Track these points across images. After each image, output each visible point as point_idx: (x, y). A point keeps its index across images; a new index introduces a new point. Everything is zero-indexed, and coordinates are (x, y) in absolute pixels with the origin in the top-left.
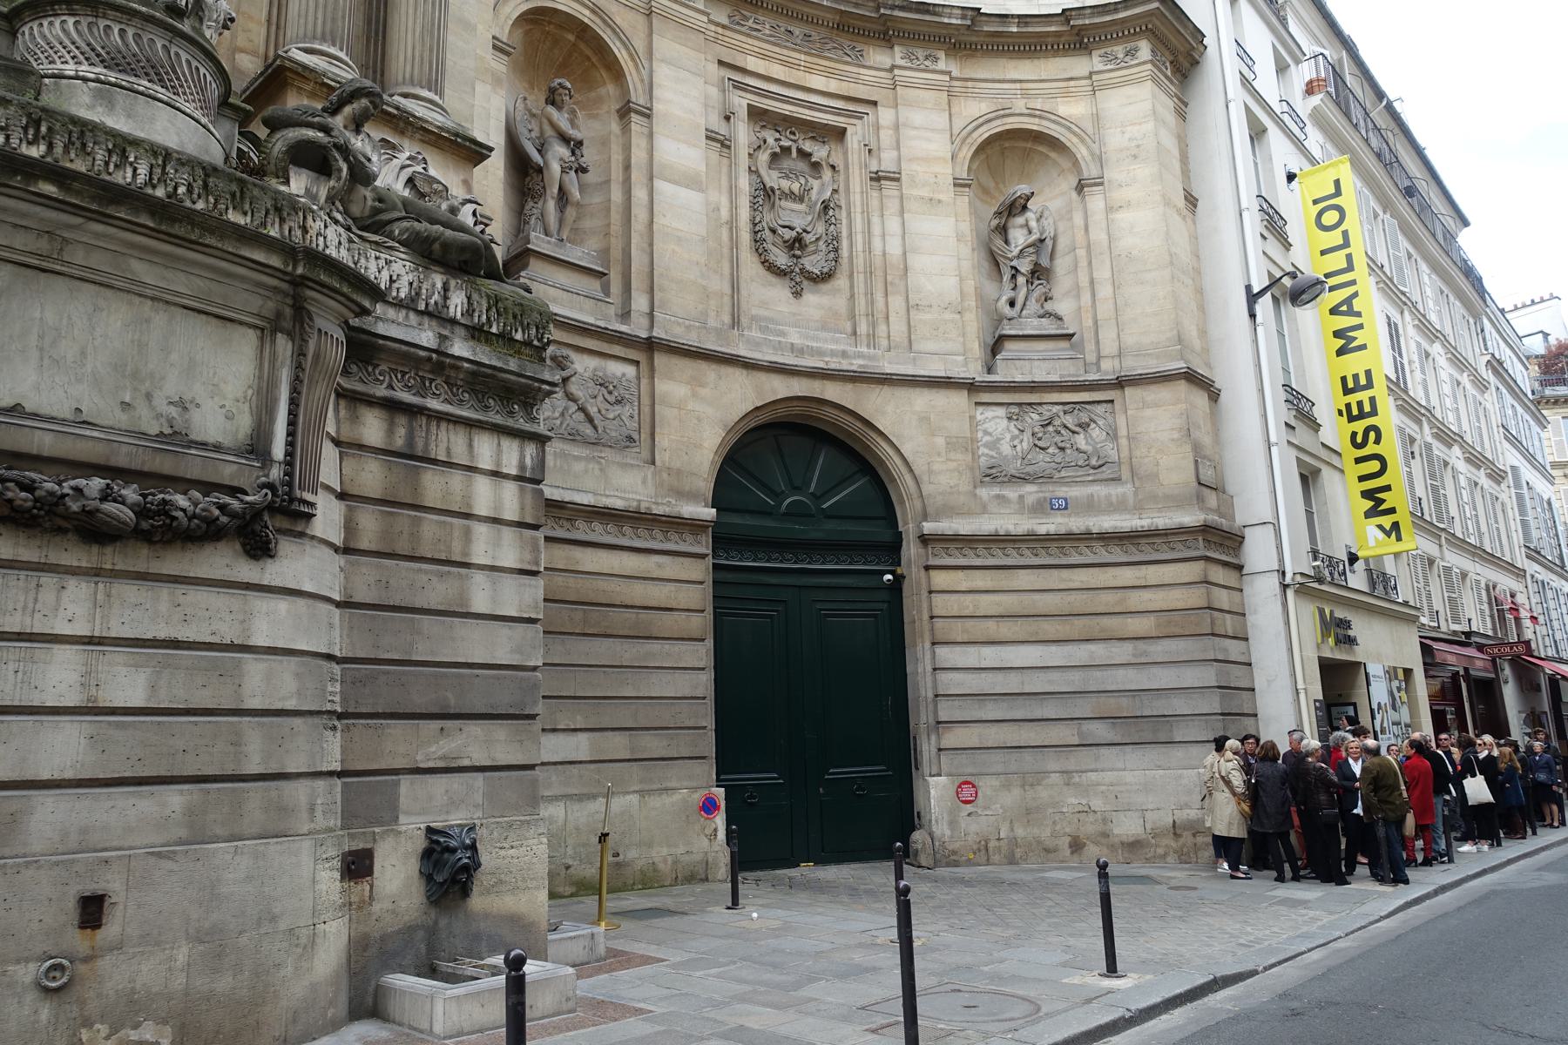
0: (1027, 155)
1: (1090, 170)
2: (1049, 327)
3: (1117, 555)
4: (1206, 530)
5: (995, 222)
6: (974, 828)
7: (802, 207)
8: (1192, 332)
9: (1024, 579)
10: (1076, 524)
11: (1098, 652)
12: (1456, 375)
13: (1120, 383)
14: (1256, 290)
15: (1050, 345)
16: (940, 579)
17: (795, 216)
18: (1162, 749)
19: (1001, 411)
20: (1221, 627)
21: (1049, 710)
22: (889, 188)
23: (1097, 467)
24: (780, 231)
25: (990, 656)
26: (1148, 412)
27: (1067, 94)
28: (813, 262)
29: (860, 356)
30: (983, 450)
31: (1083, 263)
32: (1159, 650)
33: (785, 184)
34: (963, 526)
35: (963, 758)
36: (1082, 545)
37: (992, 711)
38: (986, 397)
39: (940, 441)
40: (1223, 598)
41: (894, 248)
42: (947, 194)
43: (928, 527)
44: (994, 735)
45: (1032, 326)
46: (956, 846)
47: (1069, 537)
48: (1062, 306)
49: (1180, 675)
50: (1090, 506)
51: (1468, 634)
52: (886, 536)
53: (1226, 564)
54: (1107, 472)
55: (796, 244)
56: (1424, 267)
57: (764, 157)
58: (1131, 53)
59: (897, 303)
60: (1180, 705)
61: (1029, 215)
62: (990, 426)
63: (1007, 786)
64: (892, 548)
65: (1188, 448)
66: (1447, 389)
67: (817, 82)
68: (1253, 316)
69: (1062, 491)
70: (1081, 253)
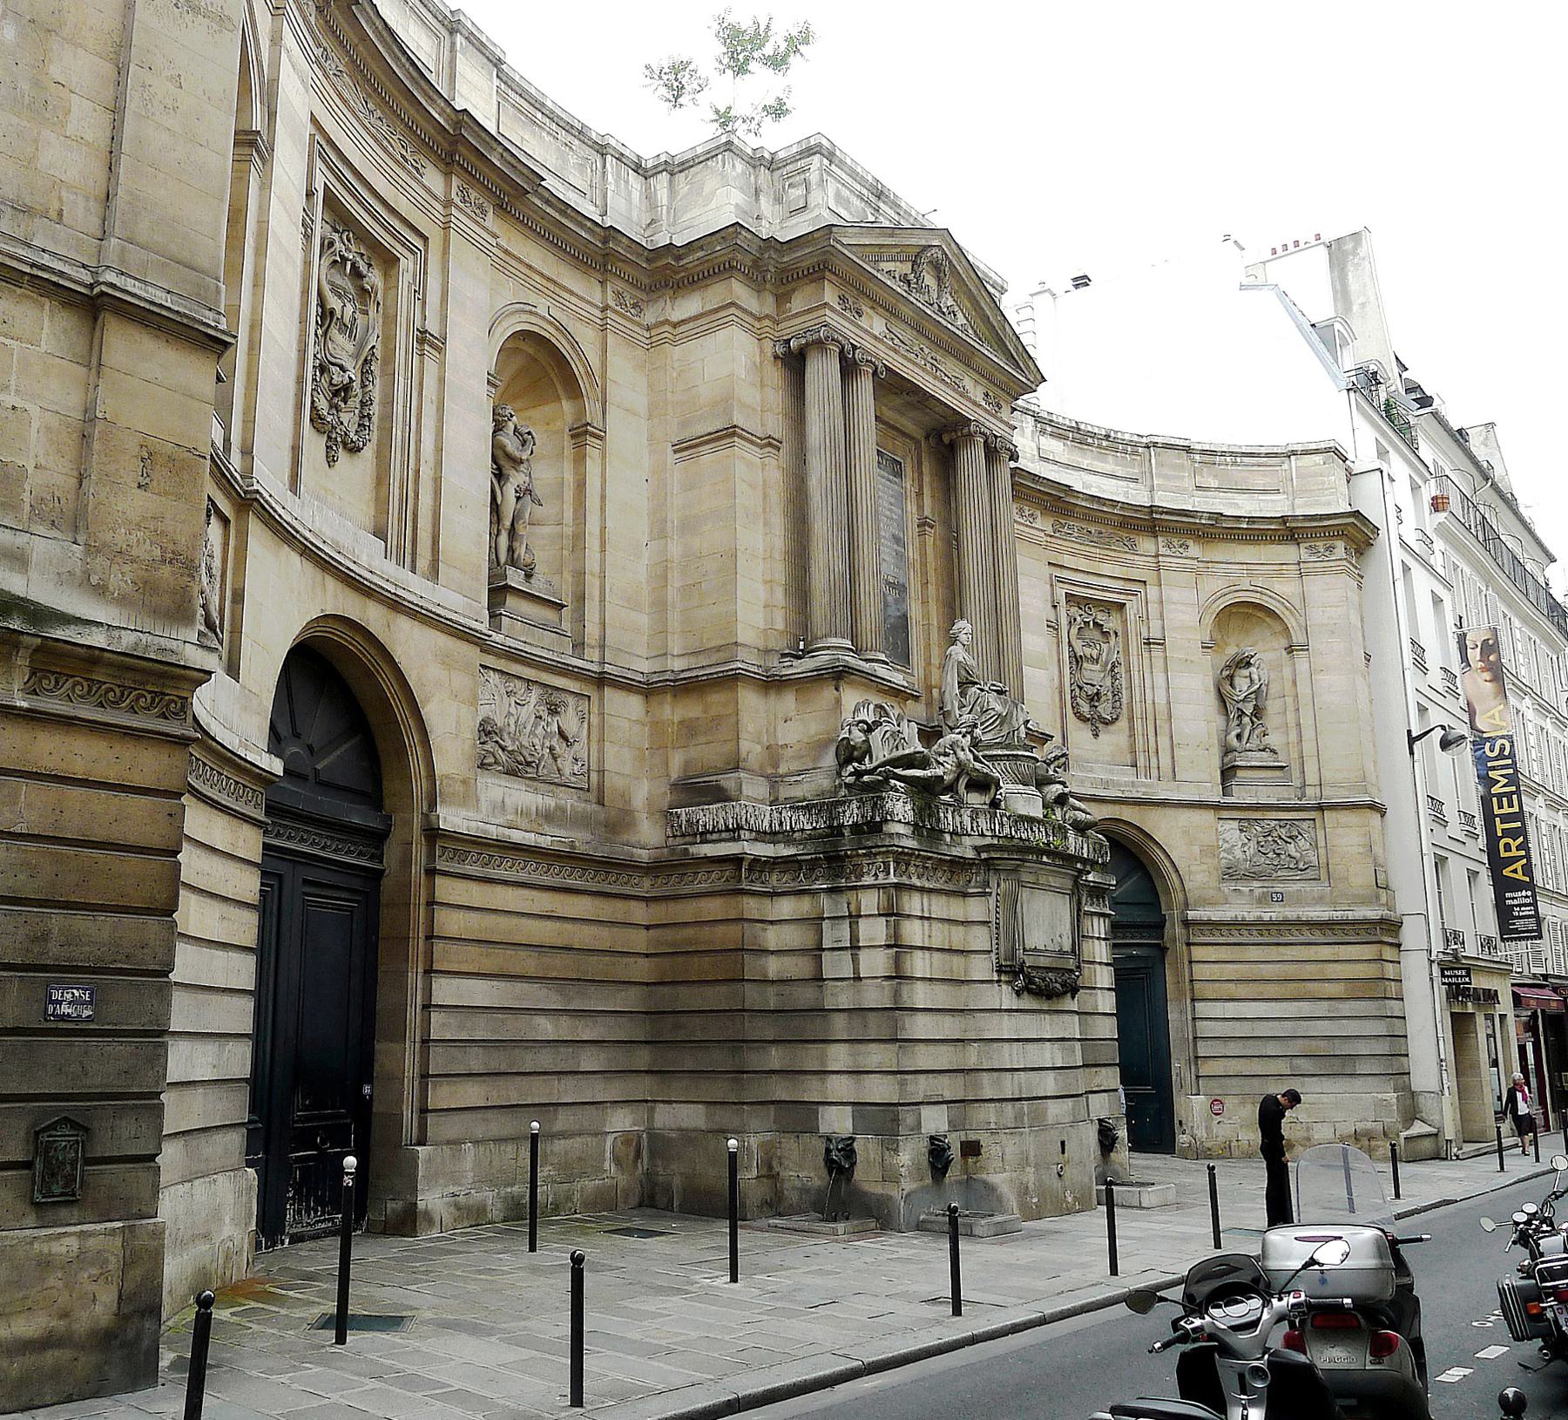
0: (1249, 616)
1: (1298, 638)
2: (1265, 759)
3: (1318, 937)
4: (1382, 921)
5: (1226, 673)
6: (1221, 1133)
7: (1098, 667)
8: (1370, 767)
9: (1253, 953)
10: (1290, 913)
11: (1305, 1008)
12: (1541, 722)
13: (1321, 808)
14: (1414, 734)
15: (1269, 773)
16: (1198, 953)
17: (1093, 673)
18: (1348, 1079)
19: (1235, 824)
20: (1380, 990)
21: (1272, 1049)
22: (1157, 652)
23: (1300, 868)
24: (1086, 688)
25: (1231, 1009)
26: (1340, 831)
27: (1280, 574)
28: (1104, 709)
29: (1145, 785)
30: (1223, 854)
31: (1291, 708)
32: (1346, 1008)
33: (1088, 651)
34: (1215, 915)
35: (1213, 1083)
36: (1293, 929)
37: (1234, 1049)
38: (1225, 814)
39: (1196, 849)
40: (1390, 971)
41: (1161, 700)
42: (1197, 653)
43: (1191, 915)
44: (1235, 1067)
45: (1257, 759)
46: (1207, 1145)
47: (1286, 923)
48: (1273, 740)
49: (1356, 1025)
50: (1299, 900)
51: (1545, 977)
52: (1153, 919)
53: (1391, 944)
54: (1310, 874)
55: (1095, 698)
56: (1516, 623)
57: (1074, 631)
58: (1330, 549)
59: (1164, 742)
60: (1362, 1048)
61: (1253, 669)
62: (1227, 836)
63: (1243, 1103)
64: (1159, 926)
65: (1370, 860)
66: (1532, 740)
67: (1107, 569)
68: (1412, 753)
69: (1279, 887)
70: (1289, 700)
